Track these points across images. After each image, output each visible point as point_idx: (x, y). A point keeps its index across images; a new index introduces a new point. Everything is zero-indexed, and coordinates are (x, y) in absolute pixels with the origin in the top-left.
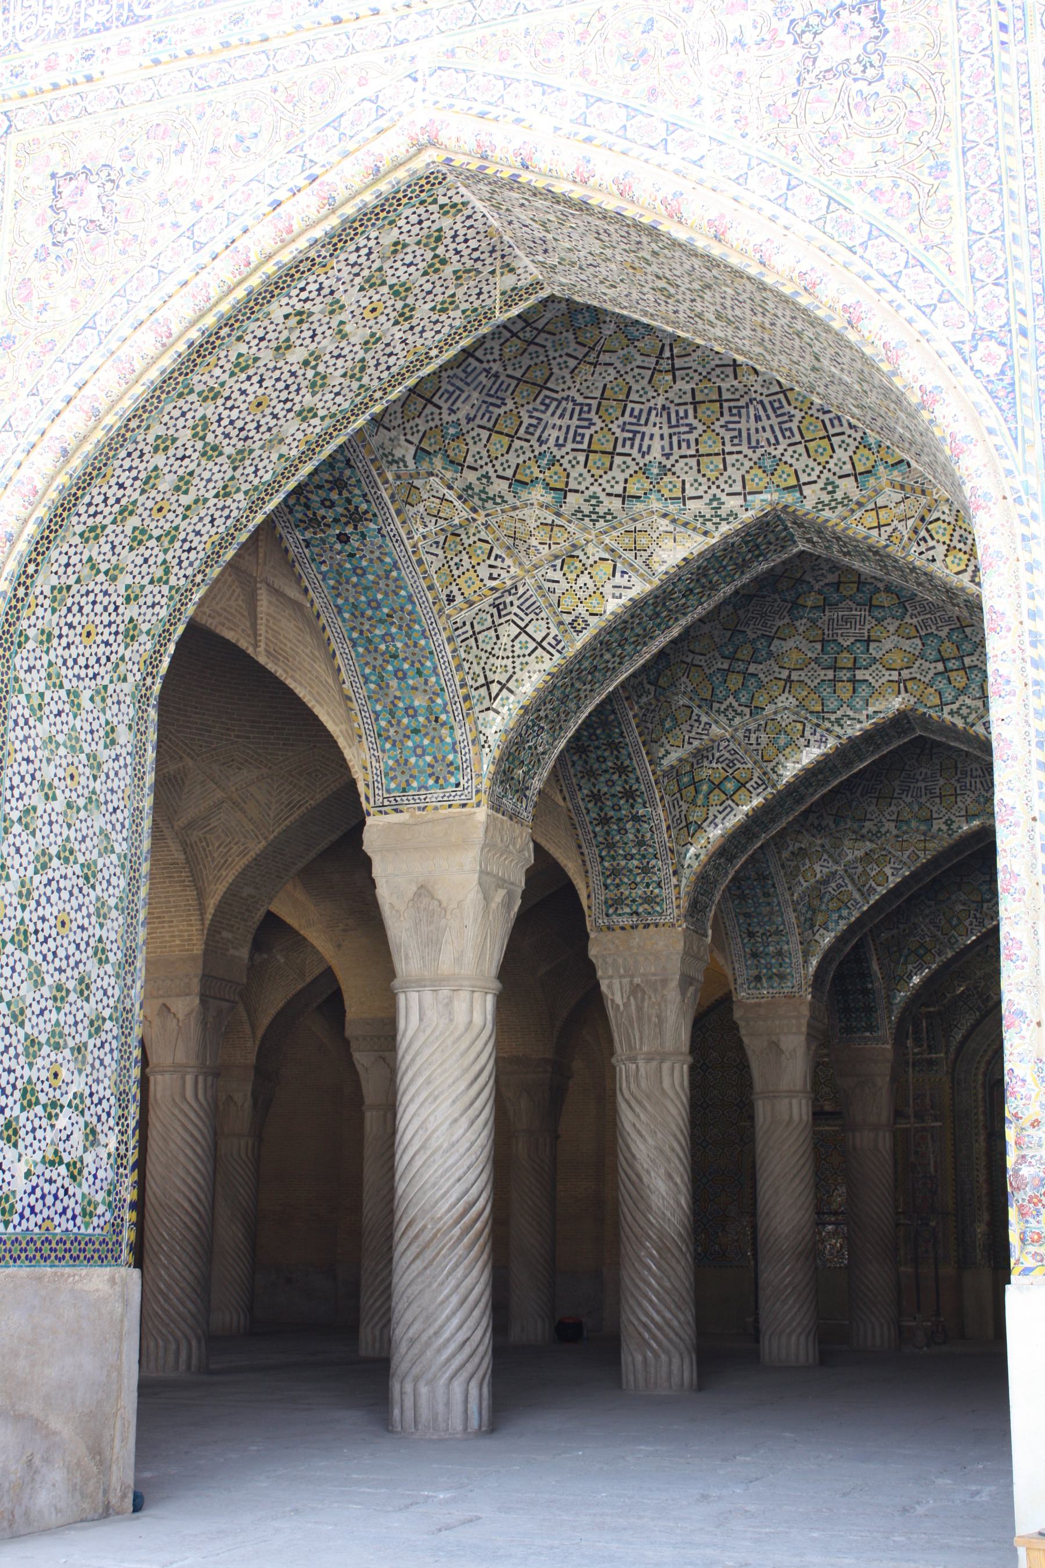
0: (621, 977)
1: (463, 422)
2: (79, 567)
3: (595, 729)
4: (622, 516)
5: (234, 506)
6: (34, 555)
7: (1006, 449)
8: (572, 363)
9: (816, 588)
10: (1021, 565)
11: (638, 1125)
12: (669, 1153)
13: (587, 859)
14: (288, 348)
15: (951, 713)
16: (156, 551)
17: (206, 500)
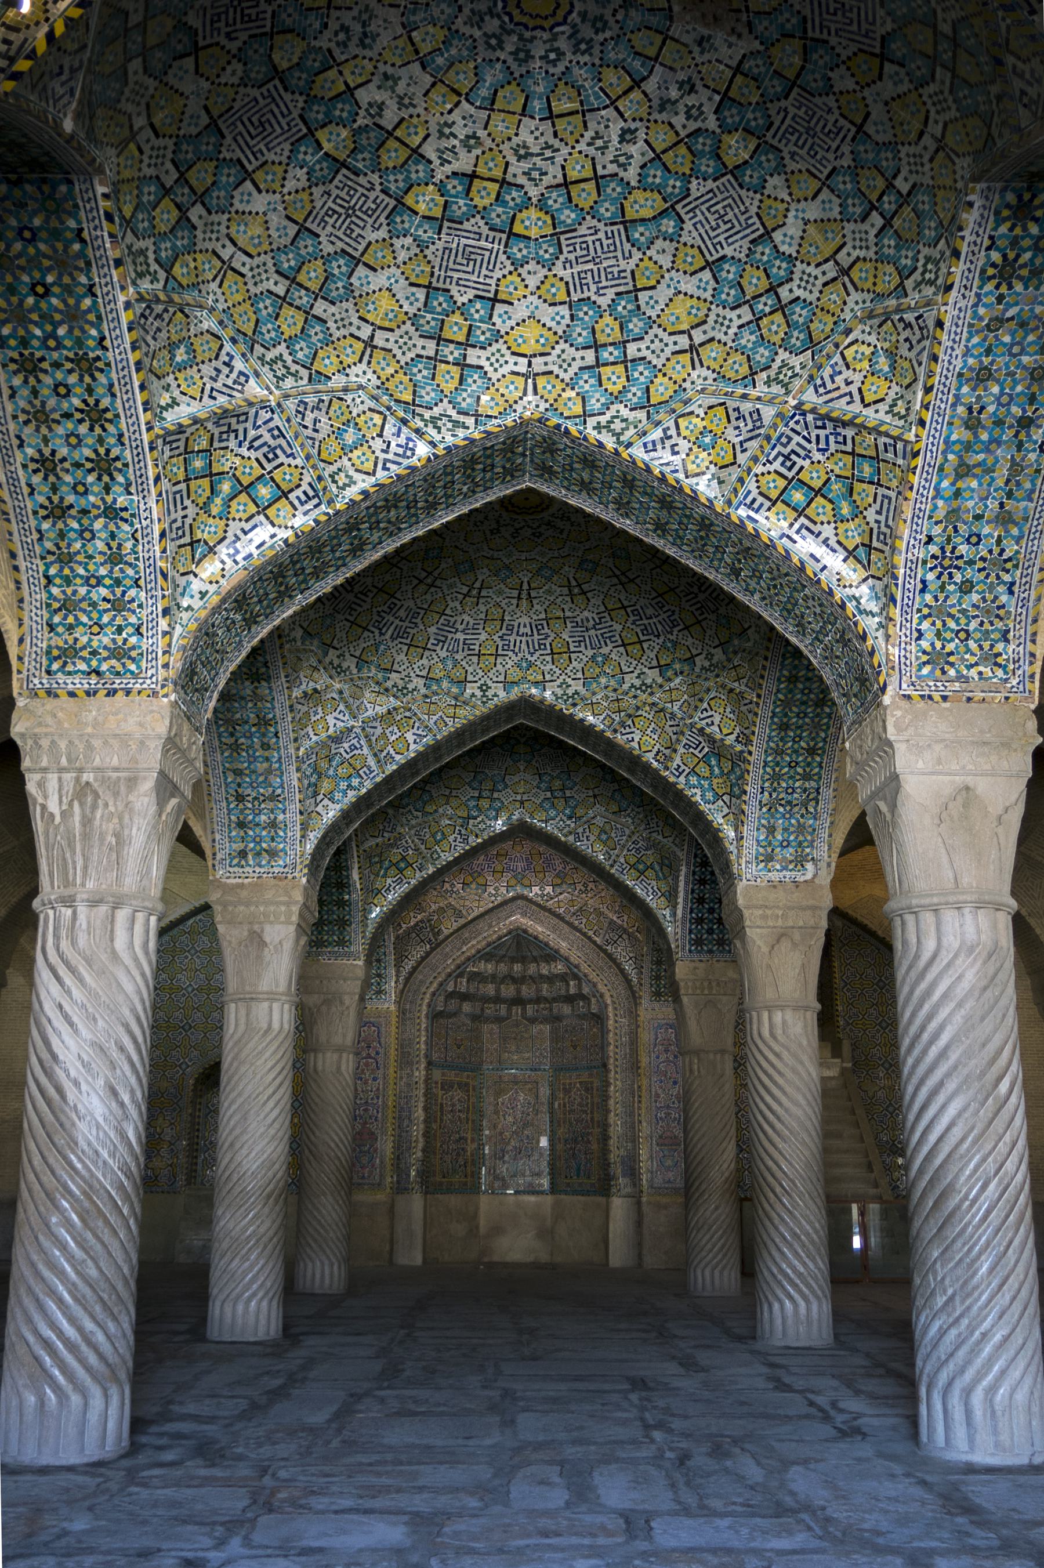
0: (61, 770)
3: (56, 325)
9: (439, 176)
11: (67, 1007)
12: (115, 1054)
13: (23, 578)
15: (598, 427)
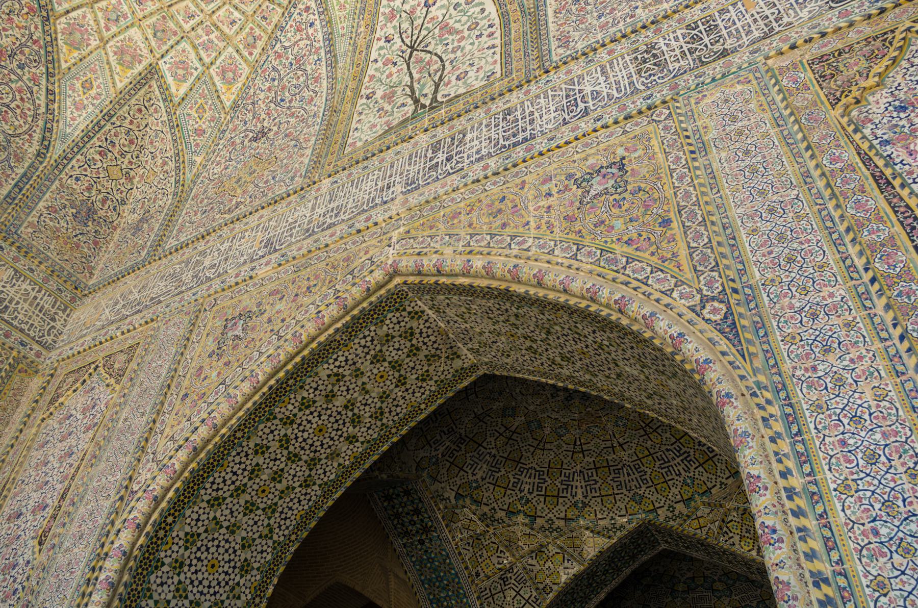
1: (480, 480)
2: (206, 522)
4: (565, 529)
5: (313, 493)
6: (172, 511)
7: (738, 363)
8: (532, 449)
10: (767, 440)
14: (333, 396)
16: (262, 517)
17: (294, 488)
